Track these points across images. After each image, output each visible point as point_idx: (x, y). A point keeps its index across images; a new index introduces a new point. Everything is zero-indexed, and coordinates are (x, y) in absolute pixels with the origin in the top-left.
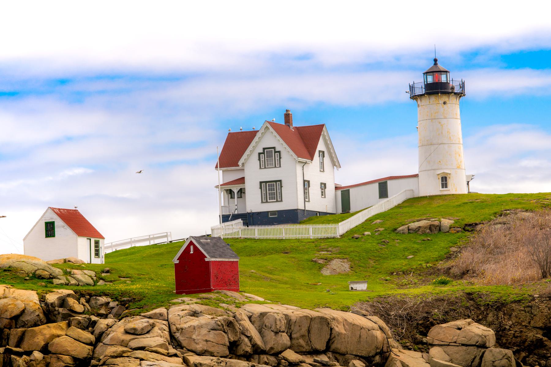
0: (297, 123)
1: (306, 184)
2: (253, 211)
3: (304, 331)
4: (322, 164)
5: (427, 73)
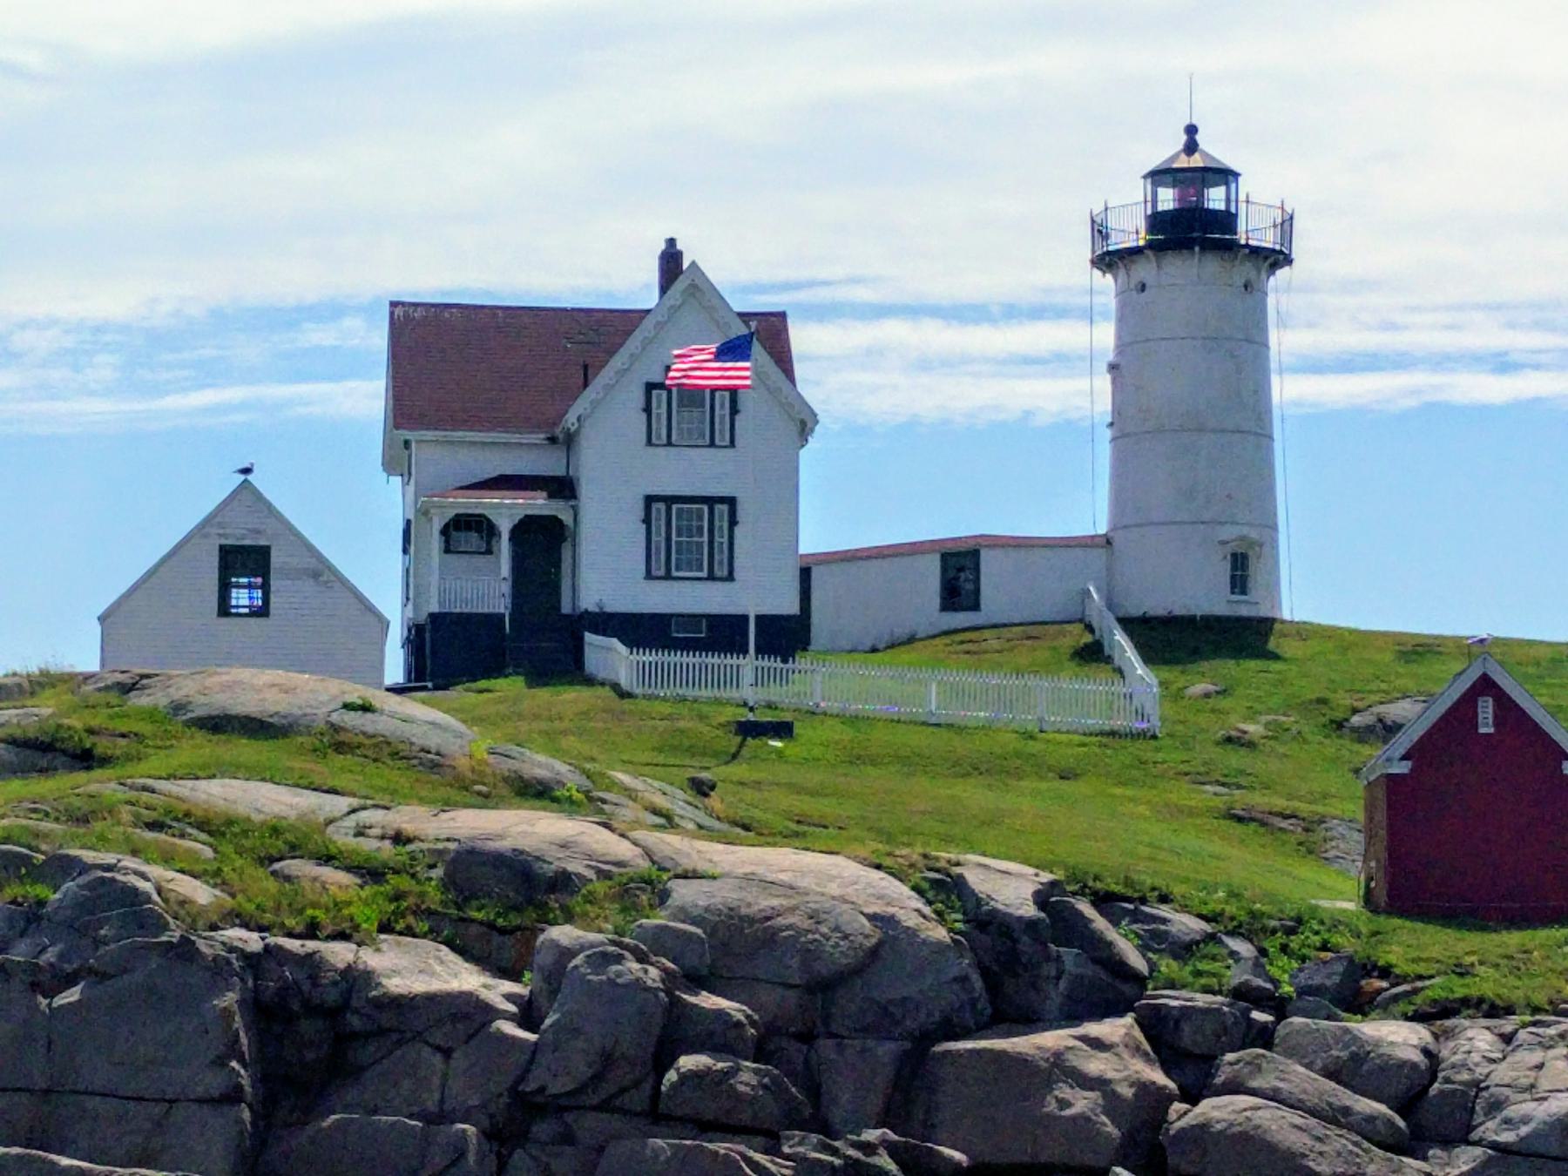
2: (608, 609)
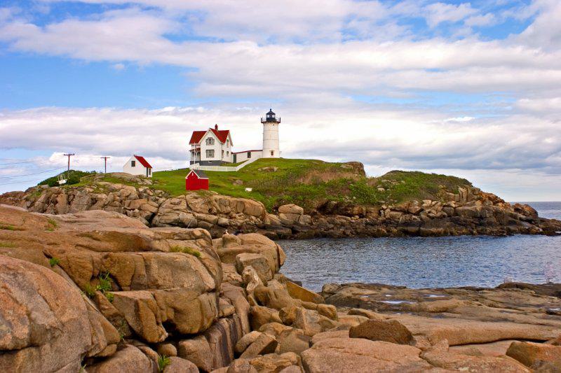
0: (219, 129)
1: (223, 151)
3: (235, 205)
4: (228, 144)
5: (267, 114)
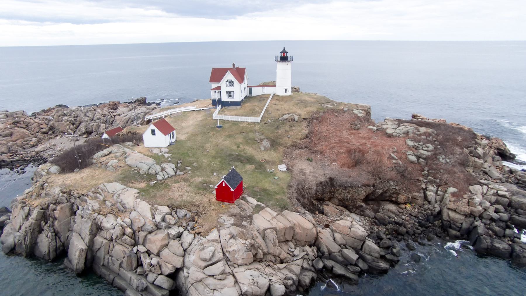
3: (283, 234)
